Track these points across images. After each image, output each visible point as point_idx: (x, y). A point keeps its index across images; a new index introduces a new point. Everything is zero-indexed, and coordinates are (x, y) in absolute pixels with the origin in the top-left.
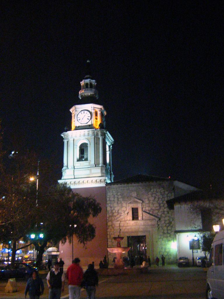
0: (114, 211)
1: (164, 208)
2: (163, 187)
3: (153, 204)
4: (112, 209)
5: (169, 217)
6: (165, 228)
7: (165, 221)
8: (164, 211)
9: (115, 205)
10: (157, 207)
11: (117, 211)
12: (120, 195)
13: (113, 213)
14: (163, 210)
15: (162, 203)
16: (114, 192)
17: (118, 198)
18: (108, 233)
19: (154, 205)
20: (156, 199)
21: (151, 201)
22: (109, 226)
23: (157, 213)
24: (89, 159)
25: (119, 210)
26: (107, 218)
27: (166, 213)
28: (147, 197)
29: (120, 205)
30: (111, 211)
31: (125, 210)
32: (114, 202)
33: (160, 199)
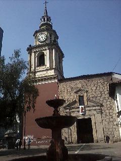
9: (65, 94)
20: (98, 88)
27: (107, 98)
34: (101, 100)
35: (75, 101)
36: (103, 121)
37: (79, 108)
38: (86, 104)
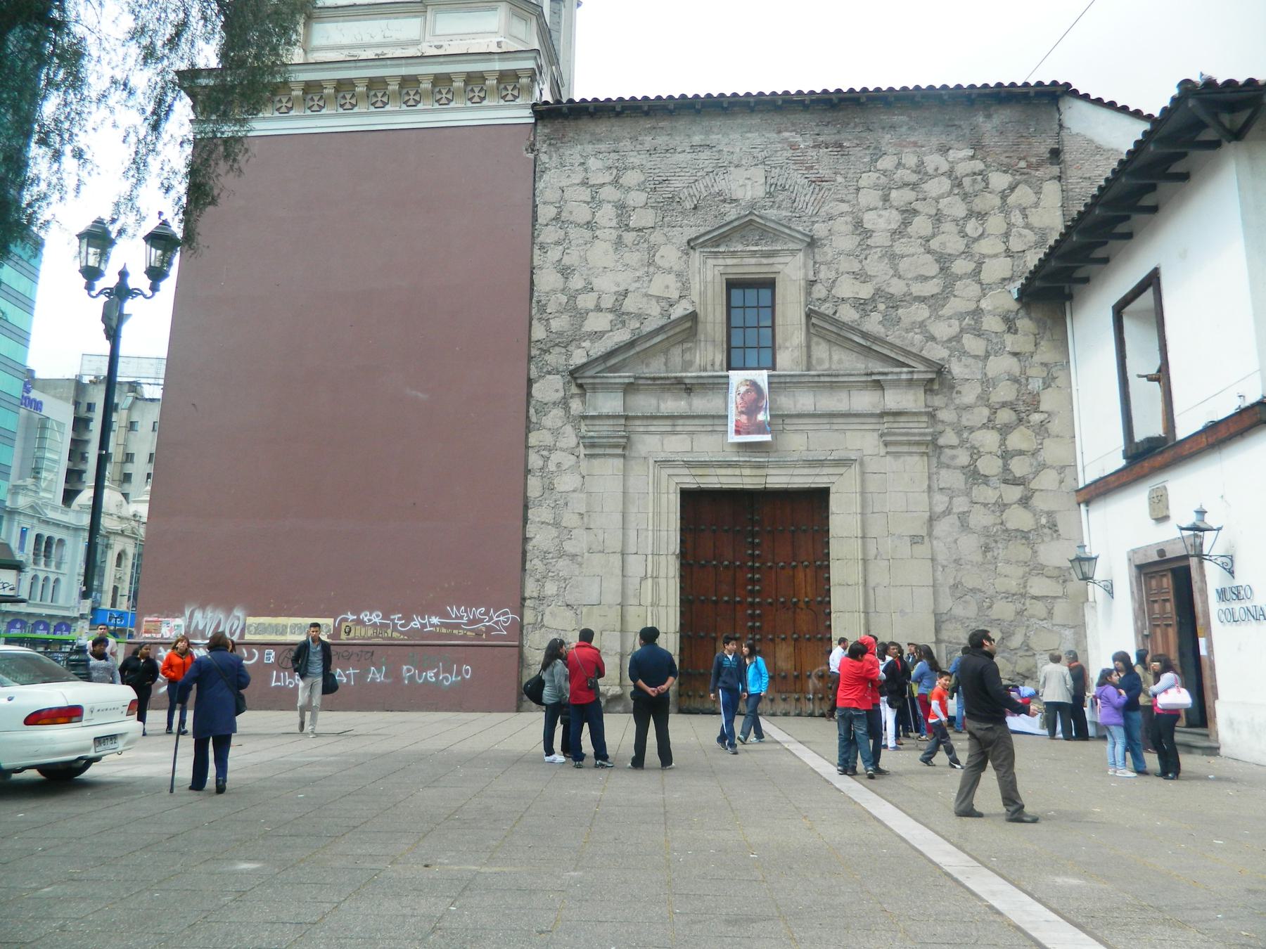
0: (586, 301)
1: (975, 289)
2: (977, 146)
3: (893, 258)
4: (576, 282)
5: (1015, 354)
6: (989, 440)
7: (988, 383)
8: (977, 313)
9: (601, 253)
10: (925, 279)
11: (608, 302)
12: (641, 187)
13: (582, 315)
14: (972, 306)
15: (966, 253)
16: (593, 163)
17: (621, 207)
18: (534, 461)
19: (903, 265)
20: (921, 225)
21: (880, 239)
22: (543, 408)
23: (922, 324)
25: (626, 292)
27: (992, 324)
28: (844, 207)
29: (633, 258)
30: (564, 299)
31: (675, 295)
32: (588, 234)
33: (948, 227)
34: (942, 330)
35: (693, 317)
36: (942, 527)
37: (720, 385)
38: (787, 360)
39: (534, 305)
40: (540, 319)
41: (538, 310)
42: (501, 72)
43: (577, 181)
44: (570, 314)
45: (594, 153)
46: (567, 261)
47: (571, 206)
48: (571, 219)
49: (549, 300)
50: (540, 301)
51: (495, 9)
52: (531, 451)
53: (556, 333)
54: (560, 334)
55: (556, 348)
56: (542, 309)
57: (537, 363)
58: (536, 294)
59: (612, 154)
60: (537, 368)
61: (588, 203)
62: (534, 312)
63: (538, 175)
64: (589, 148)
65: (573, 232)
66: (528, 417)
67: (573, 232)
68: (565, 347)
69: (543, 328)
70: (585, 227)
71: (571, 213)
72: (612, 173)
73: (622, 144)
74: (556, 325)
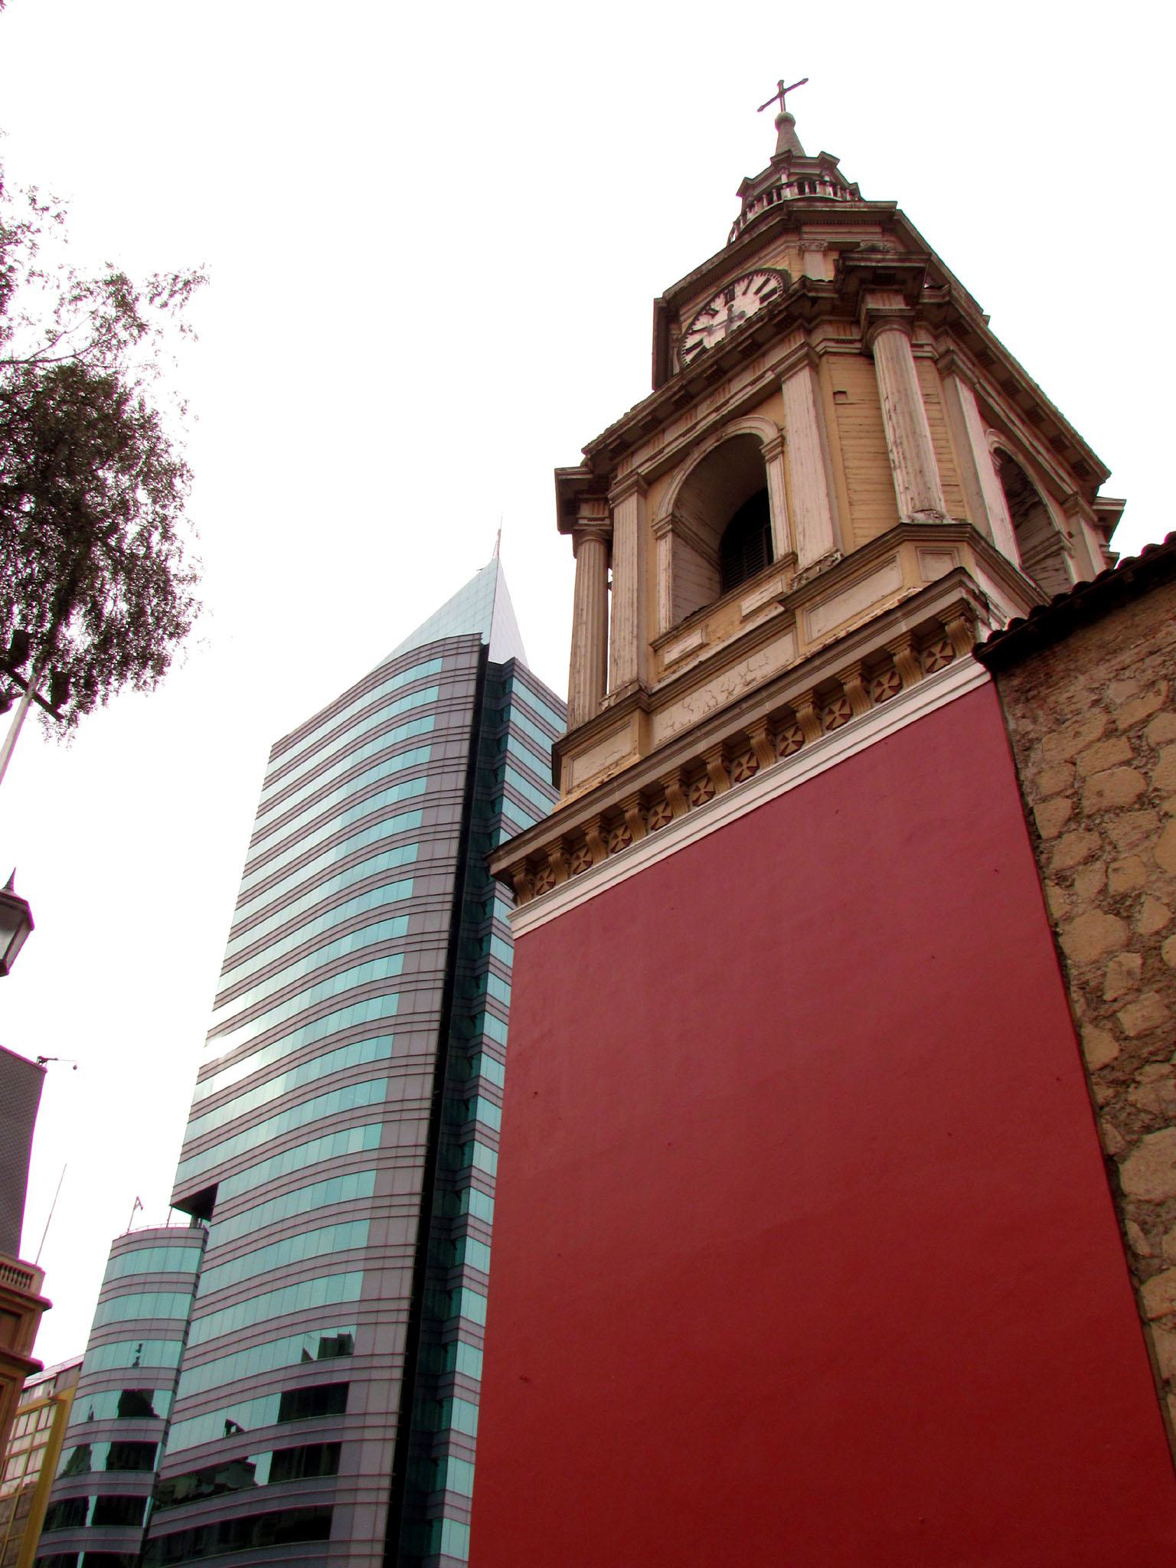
16: (1116, 692)
24: (780, 548)
26: (1103, 1093)
30: (1134, 961)
32: (1146, 819)
39: (1075, 996)
40: (1095, 1022)
41: (1088, 1003)
42: (913, 632)
43: (1097, 732)
44: (1156, 986)
45: (1111, 675)
46: (1118, 885)
47: (1094, 783)
48: (1105, 803)
49: (1104, 975)
50: (1087, 983)
51: (893, 560)
52: (1156, 1331)
53: (1138, 1037)
54: (1144, 1036)
55: (1148, 1068)
56: (1095, 997)
57: (1114, 1117)
58: (1074, 972)
59: (1147, 661)
60: (1116, 1127)
61: (1127, 763)
62: (1079, 1008)
63: (1020, 758)
64: (1102, 672)
65: (1119, 830)
66: (1127, 1247)
67: (1119, 830)
68: (1167, 1060)
69: (1106, 1037)
70: (1137, 806)
71: (1100, 794)
72: (1159, 690)
73: (1160, 635)
74: (1131, 1020)
